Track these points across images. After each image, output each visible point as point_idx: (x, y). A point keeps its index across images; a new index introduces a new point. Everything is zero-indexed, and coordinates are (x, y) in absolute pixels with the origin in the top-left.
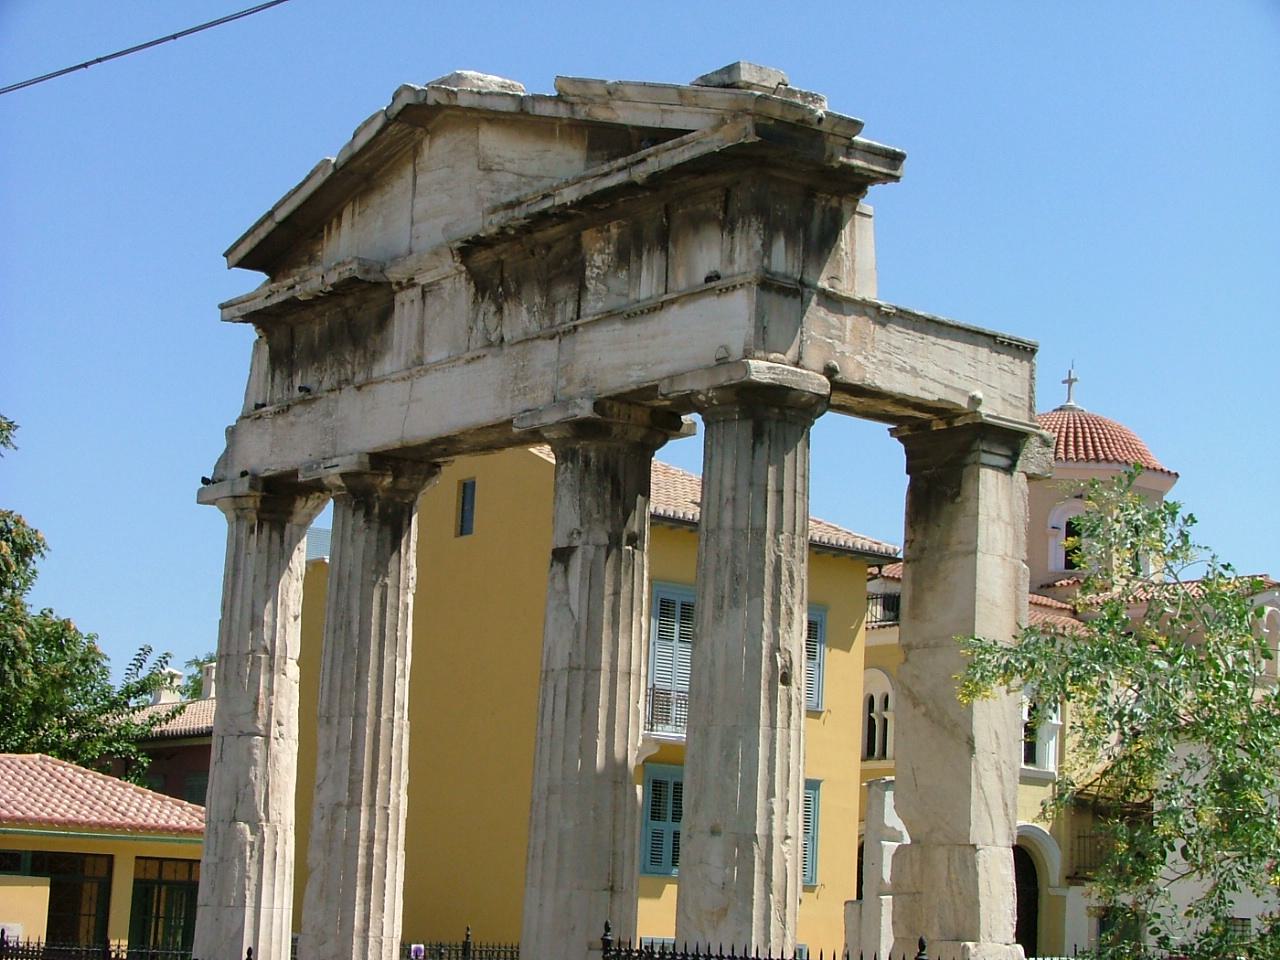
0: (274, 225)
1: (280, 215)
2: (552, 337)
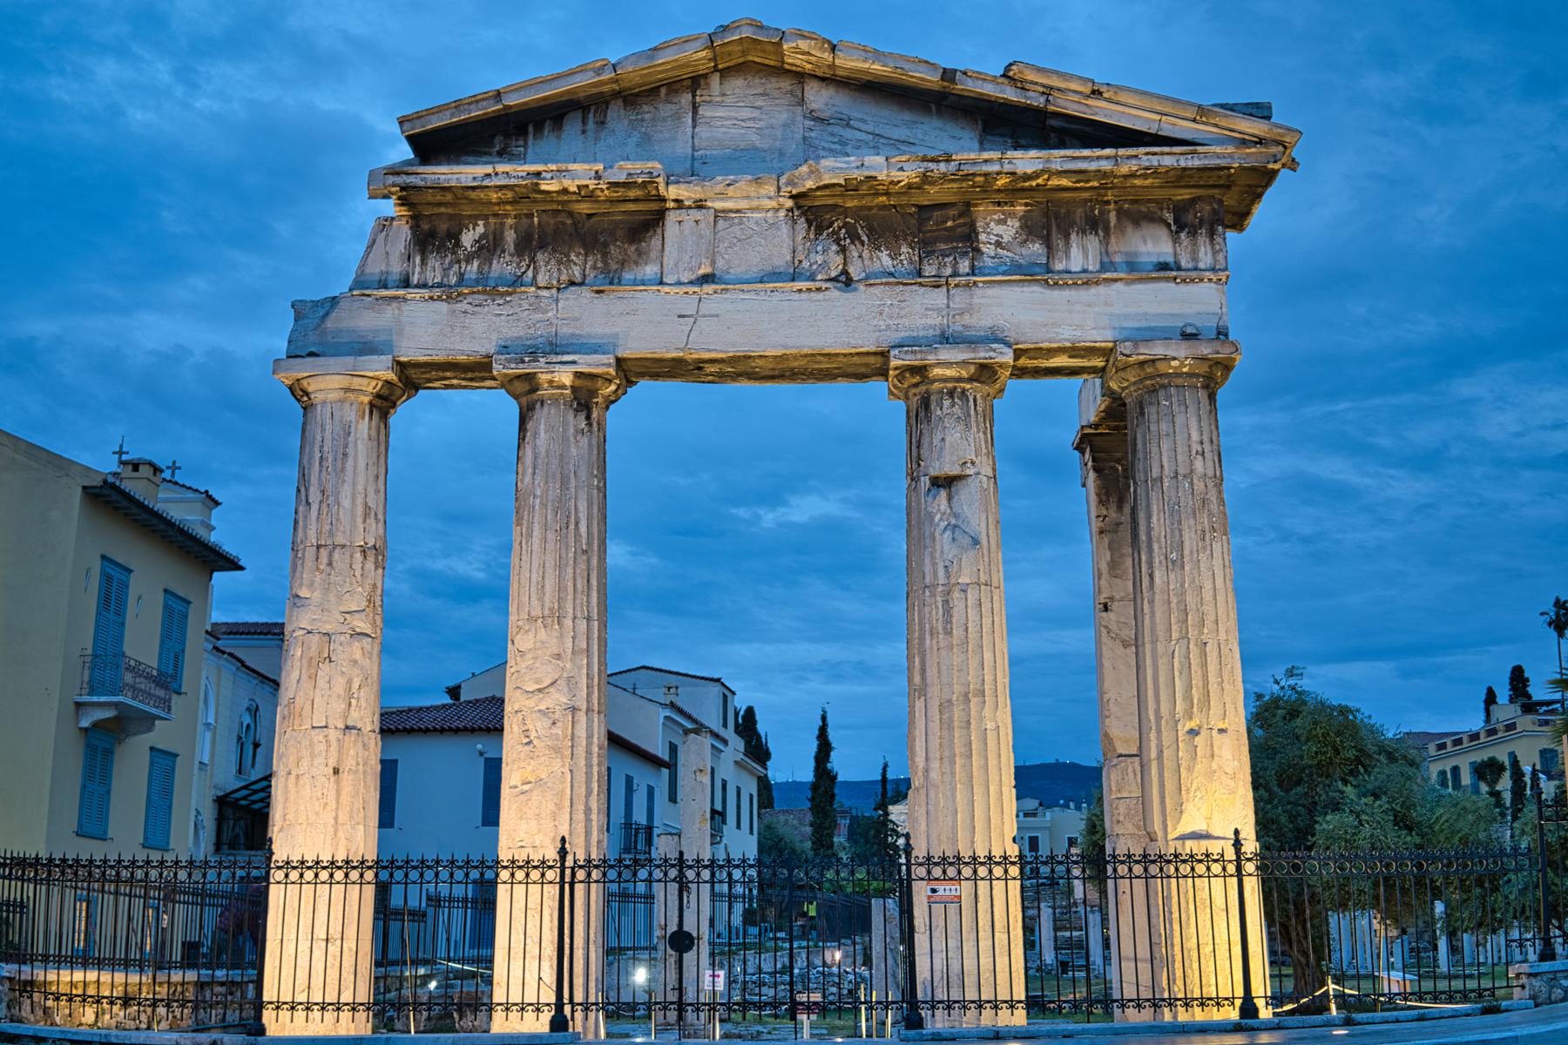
1: (512, 100)
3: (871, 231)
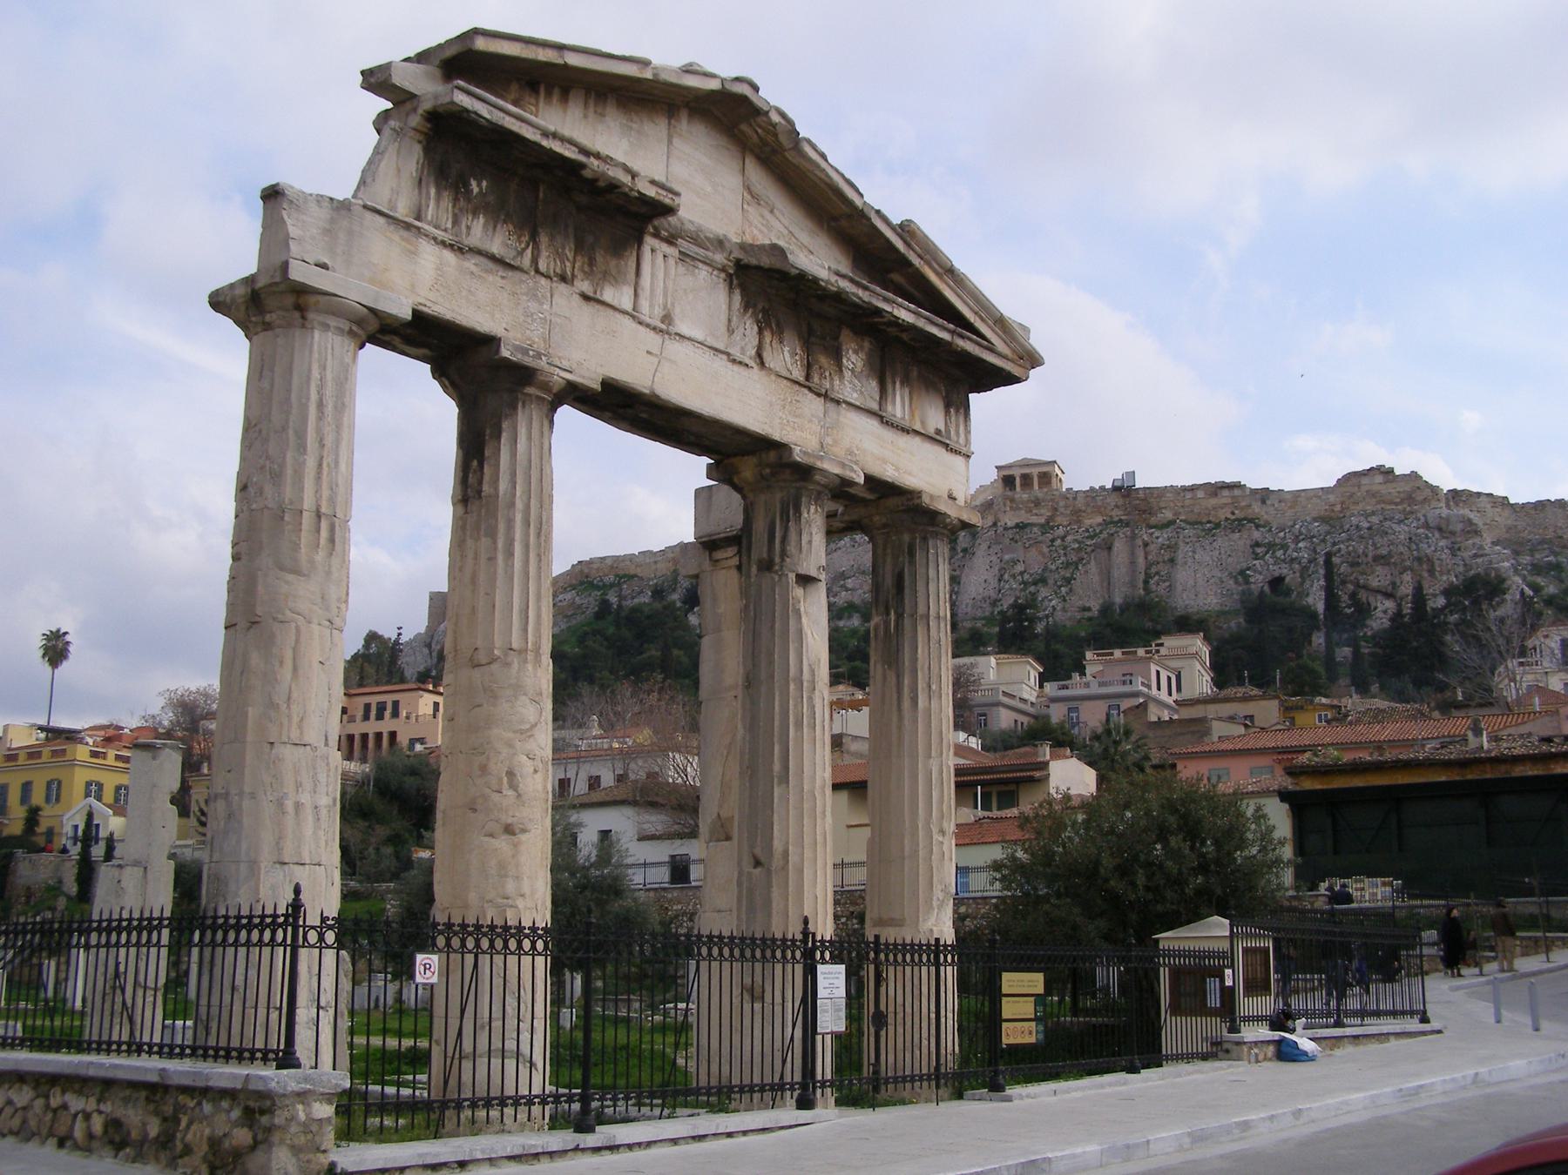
0: (560, 61)
1: (573, 60)
2: (819, 395)
3: (778, 325)
